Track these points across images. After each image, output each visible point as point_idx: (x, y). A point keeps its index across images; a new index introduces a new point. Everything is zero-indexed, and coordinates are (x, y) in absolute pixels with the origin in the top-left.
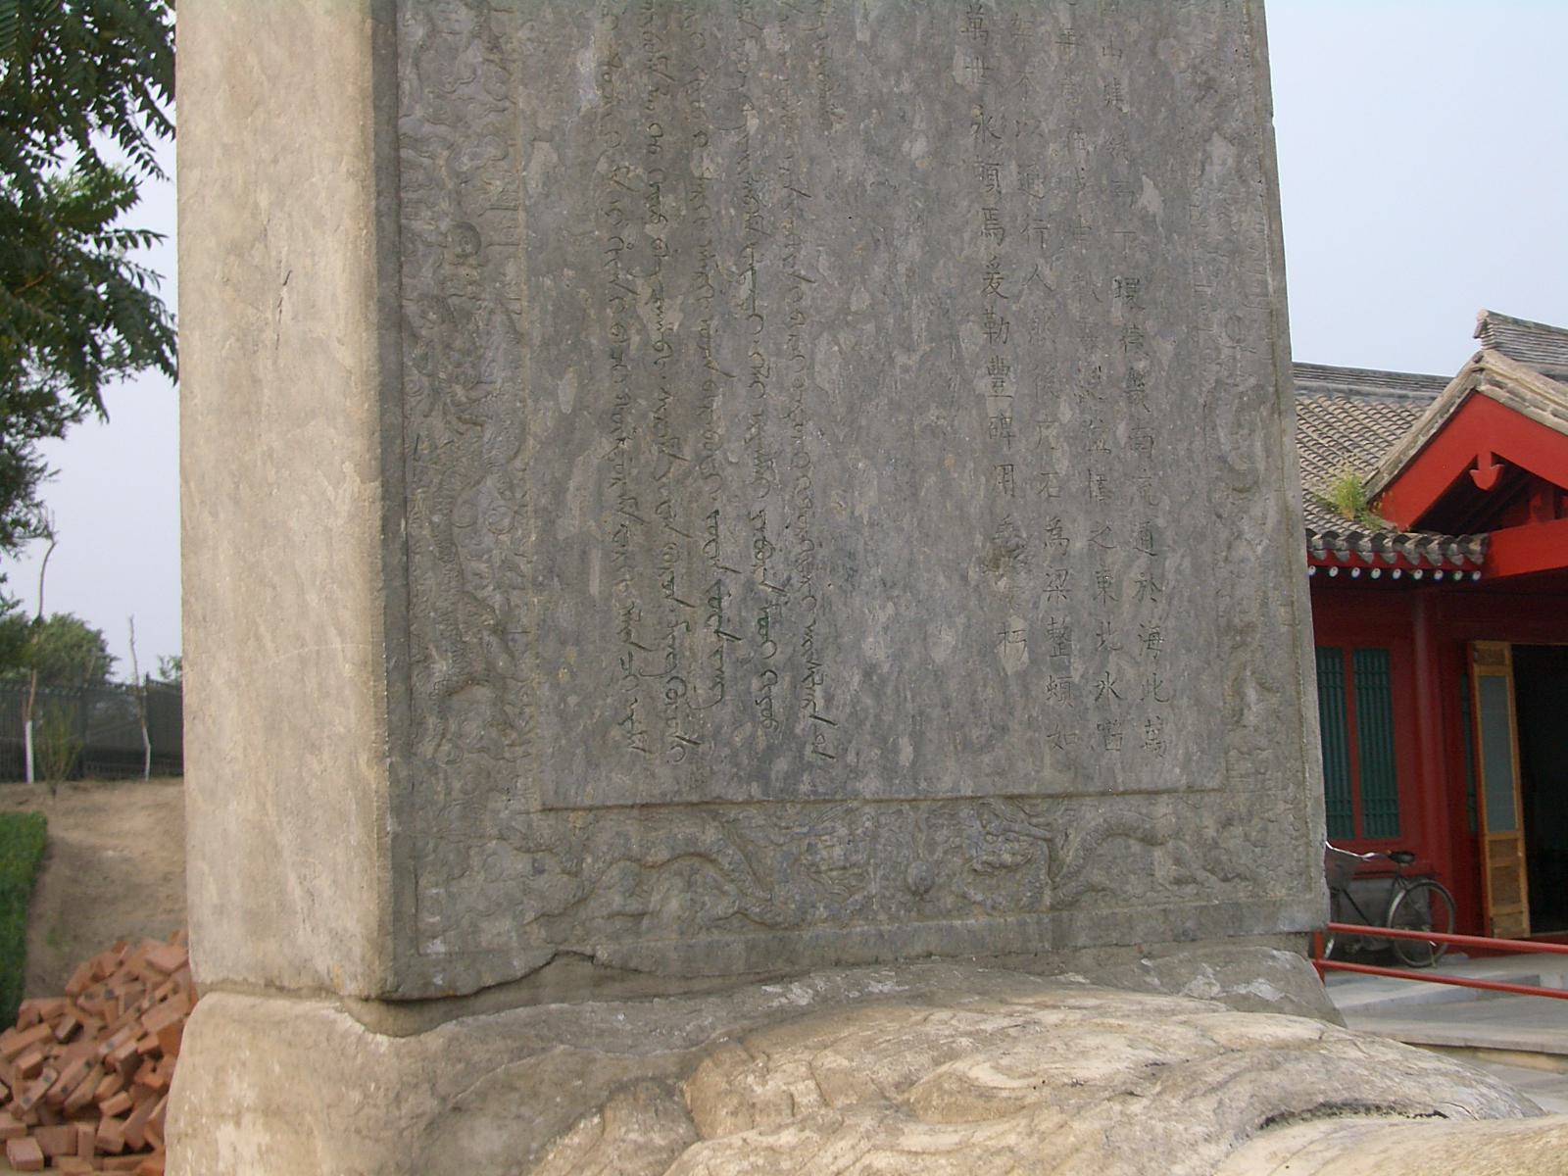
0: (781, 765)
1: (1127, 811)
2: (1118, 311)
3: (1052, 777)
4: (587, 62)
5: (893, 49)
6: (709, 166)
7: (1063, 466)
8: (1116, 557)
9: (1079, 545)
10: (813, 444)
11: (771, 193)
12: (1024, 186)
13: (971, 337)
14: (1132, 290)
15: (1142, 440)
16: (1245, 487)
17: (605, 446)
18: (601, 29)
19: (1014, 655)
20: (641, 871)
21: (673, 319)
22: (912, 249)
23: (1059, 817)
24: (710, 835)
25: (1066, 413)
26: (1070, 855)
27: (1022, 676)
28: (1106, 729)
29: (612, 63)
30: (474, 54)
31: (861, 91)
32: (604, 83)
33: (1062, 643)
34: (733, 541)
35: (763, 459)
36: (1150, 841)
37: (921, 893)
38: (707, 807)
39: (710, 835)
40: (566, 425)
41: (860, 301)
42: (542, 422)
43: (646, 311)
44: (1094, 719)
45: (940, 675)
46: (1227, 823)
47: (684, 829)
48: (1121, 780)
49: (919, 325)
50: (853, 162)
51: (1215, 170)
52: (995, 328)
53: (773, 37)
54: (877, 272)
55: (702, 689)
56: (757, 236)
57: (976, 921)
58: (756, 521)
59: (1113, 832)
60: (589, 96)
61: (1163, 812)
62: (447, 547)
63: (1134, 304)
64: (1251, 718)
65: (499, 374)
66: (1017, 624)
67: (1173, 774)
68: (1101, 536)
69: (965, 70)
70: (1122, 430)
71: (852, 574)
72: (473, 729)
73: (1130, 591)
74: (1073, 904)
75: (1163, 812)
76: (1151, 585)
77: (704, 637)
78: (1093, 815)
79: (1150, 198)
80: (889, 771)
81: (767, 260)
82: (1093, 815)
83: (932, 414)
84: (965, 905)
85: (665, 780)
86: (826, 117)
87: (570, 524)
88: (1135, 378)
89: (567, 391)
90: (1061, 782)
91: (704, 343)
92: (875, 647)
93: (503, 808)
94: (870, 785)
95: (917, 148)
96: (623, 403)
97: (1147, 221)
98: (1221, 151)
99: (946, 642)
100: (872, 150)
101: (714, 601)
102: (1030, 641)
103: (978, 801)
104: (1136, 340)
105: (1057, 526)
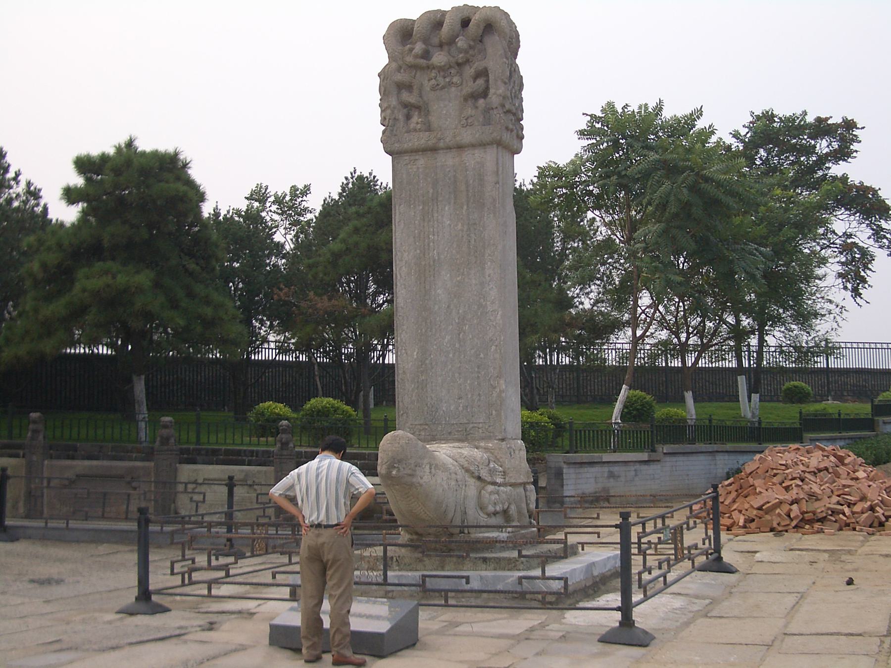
0: (434, 420)
1: (475, 425)
2: (476, 369)
3: (466, 421)
4: (415, 353)
5: (449, 346)
6: (427, 362)
7: (468, 388)
8: (474, 397)
9: (469, 396)
10: (438, 388)
11: (434, 364)
12: (464, 357)
13: (457, 375)
14: (478, 368)
15: (479, 384)
16: (495, 388)
17: (416, 391)
18: (417, 350)
19: (461, 409)
20: (420, 431)
21: (423, 378)
22: (450, 367)
23: (467, 426)
24: (427, 427)
25: (469, 382)
26: (468, 429)
27: (462, 411)
28: (472, 416)
29: (417, 353)
30: (405, 355)
31: (444, 350)
32: (417, 355)
33: (467, 407)
34: (429, 399)
35: (432, 390)
36: (479, 428)
37: (450, 433)
38: (427, 424)
39: (427, 427)
40: (413, 389)
41: (444, 373)
42: (411, 389)
43: (420, 377)
44: (471, 415)
45: (452, 411)
46: (489, 426)
47: (424, 427)
48: (475, 422)
49: (450, 374)
50: (443, 359)
51: (492, 350)
52: (460, 374)
53: (435, 347)
54: (446, 370)
55: (426, 413)
56: (432, 368)
57: (456, 436)
58: (431, 397)
59: (473, 427)
60: (415, 357)
61: (481, 425)
62: (402, 401)
63: (478, 368)
64: (494, 414)
65: (407, 385)
66: (461, 405)
67: (481, 421)
68: (472, 395)
69: (457, 346)
70: (476, 383)
71: (442, 401)
72: (405, 418)
73: (476, 401)
74: (469, 434)
75: (481, 425)
76: (479, 400)
77: (426, 408)
78: (471, 425)
79: (482, 356)
80: (446, 421)
81: (433, 370)
82: (471, 425)
83: (452, 384)
84: (455, 435)
85: (422, 422)
86: (440, 354)
87: (414, 398)
88: (478, 377)
89: (413, 386)
90: (467, 422)
91: (427, 380)
92: (444, 409)
93: (407, 425)
94: (444, 422)
95: (451, 355)
96: (418, 387)
97: (481, 358)
98: (493, 348)
99: (452, 408)
100: (445, 356)
101: (427, 405)
102: (463, 407)
103: (456, 424)
104: (479, 372)
105: (467, 394)
